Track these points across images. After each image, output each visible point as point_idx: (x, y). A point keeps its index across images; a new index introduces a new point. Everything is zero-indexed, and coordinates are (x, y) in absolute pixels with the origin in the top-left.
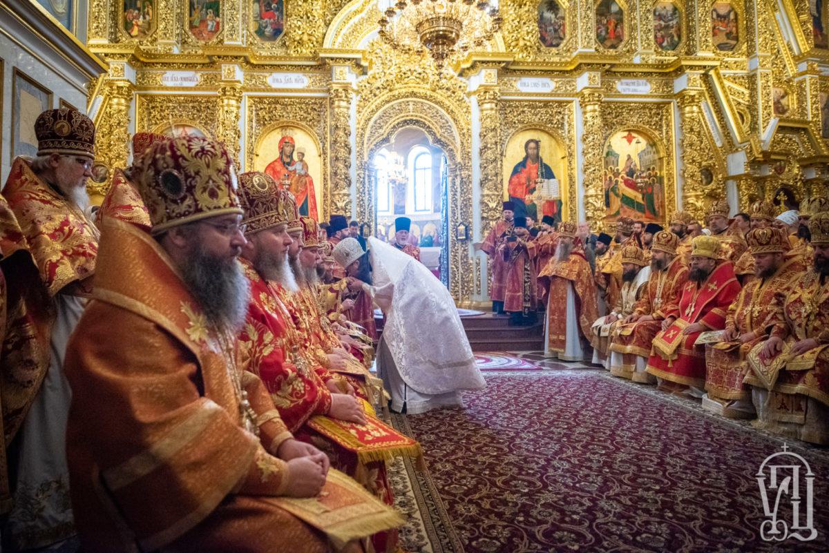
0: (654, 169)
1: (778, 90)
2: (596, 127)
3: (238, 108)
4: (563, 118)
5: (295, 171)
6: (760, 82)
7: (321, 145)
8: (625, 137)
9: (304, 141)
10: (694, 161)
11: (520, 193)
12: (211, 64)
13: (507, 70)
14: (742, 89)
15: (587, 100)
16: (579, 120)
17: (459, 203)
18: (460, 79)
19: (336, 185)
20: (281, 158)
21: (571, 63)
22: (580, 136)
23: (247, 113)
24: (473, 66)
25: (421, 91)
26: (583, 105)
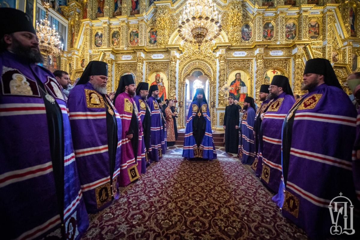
1: (335, 53)
2: (261, 68)
3: (142, 65)
5: (160, 85)
6: (327, 50)
7: (168, 77)
8: (272, 71)
9: (163, 75)
10: (298, 79)
12: (135, 52)
13: (229, 49)
14: (320, 53)
16: (255, 65)
17: (212, 95)
18: (214, 53)
19: (171, 89)
20: (156, 81)
21: (252, 45)
22: (255, 71)
23: (146, 67)
24: (217, 49)
25: (200, 58)
26: (257, 60)
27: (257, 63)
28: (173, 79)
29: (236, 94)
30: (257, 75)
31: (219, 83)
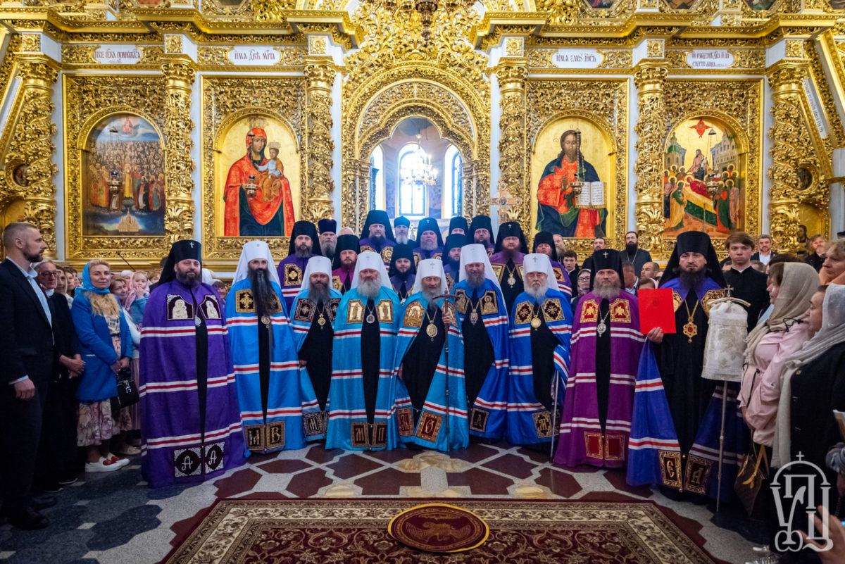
0: (731, 167)
2: (655, 113)
3: (189, 91)
4: (612, 102)
9: (277, 133)
10: (788, 158)
11: (553, 199)
15: (644, 77)
18: (479, 52)
19: (313, 189)
20: (249, 156)
23: (203, 98)
25: (428, 69)
26: (639, 84)
27: (641, 94)
28: (321, 149)
29: (563, 210)
30: (639, 139)
31: (503, 167)
